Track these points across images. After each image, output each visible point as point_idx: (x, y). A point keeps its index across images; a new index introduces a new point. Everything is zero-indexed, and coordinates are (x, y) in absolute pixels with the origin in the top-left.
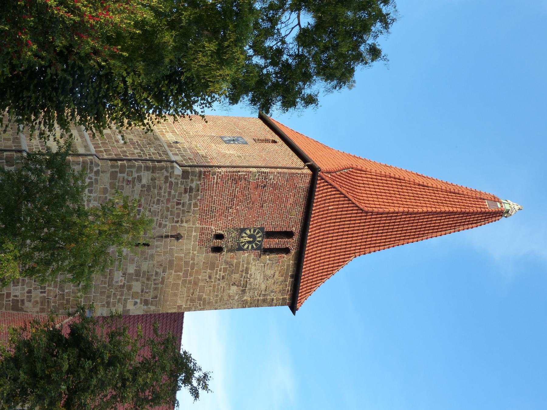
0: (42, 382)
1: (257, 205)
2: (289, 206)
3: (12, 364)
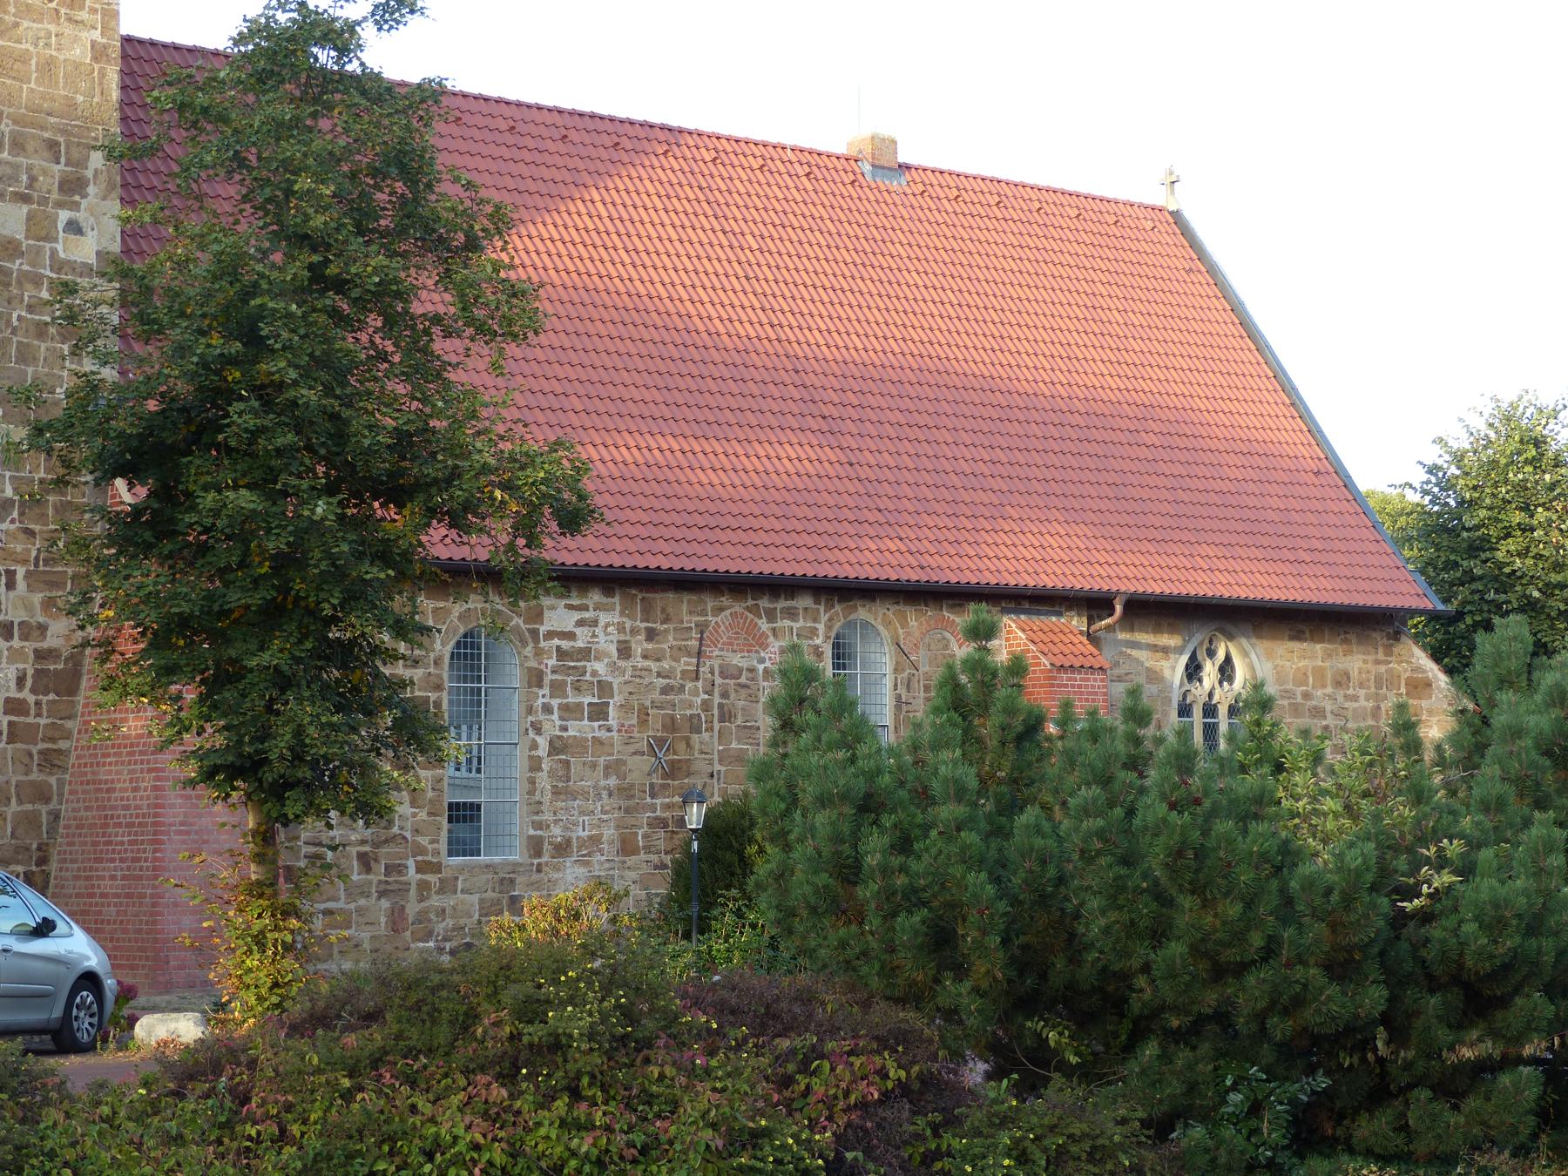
0: (298, 586)
3: (229, 695)
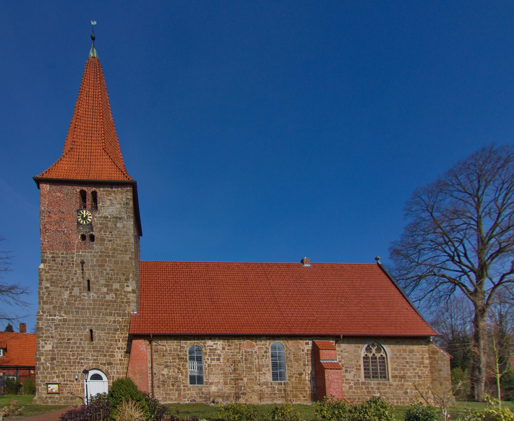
1: (63, 216)
2: (62, 195)
